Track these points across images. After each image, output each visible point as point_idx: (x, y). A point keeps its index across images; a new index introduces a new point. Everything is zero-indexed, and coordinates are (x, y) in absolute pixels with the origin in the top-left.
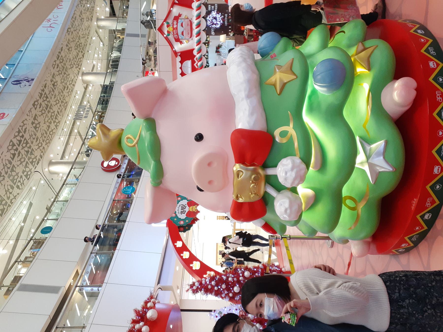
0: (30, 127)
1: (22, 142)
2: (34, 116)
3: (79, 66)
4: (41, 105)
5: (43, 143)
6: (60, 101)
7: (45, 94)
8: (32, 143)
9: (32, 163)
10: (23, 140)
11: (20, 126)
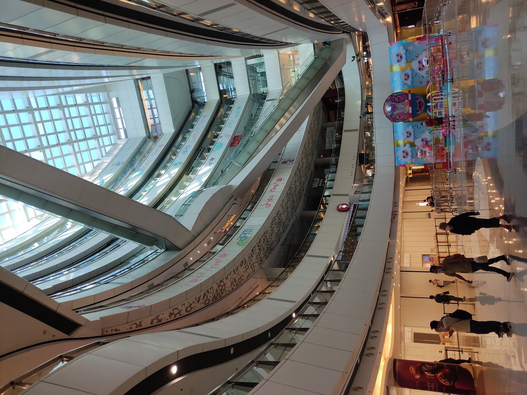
9: (294, 208)
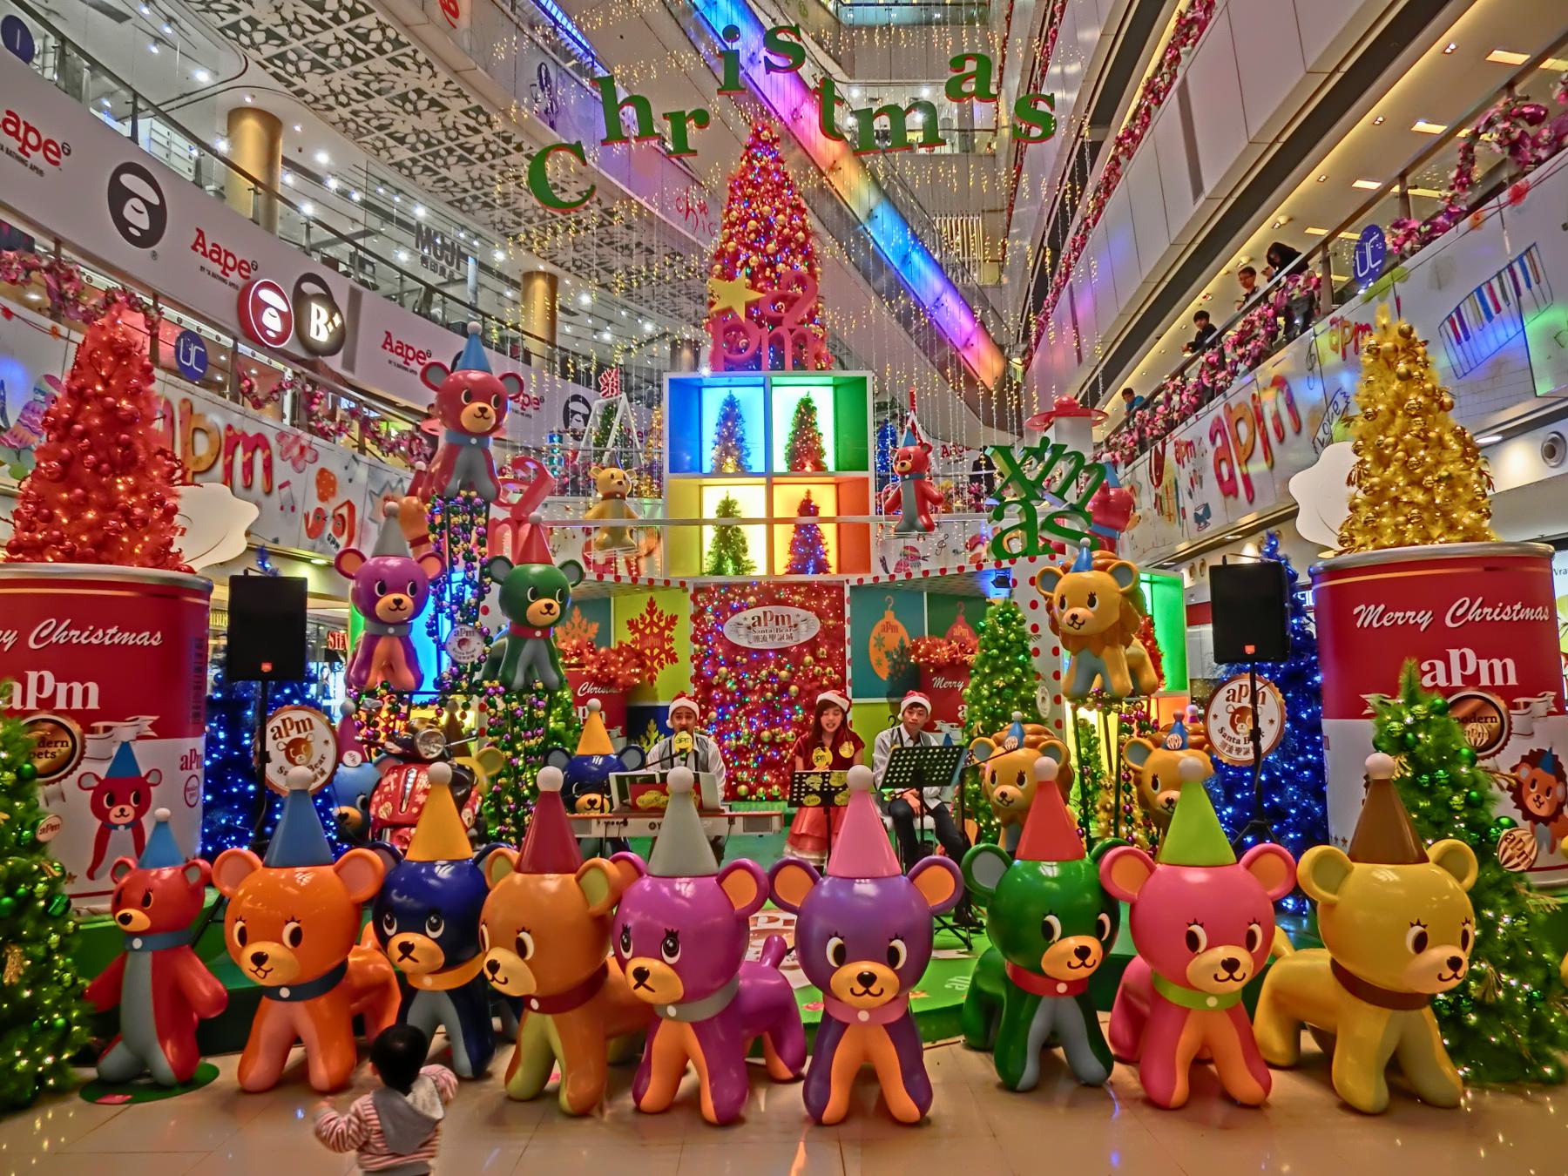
0: (408, 80)
1: (359, 44)
2: (443, 101)
3: (579, 268)
4: (476, 131)
5: (349, 109)
6: (478, 193)
7: (508, 153)
8: (355, 76)
9: (282, 57)
10: (369, 48)
11: (415, 52)
